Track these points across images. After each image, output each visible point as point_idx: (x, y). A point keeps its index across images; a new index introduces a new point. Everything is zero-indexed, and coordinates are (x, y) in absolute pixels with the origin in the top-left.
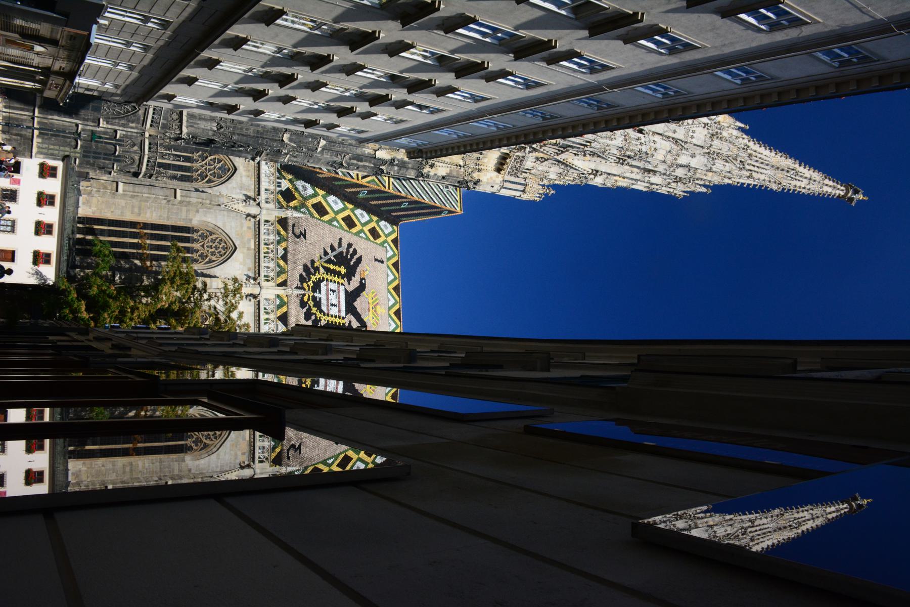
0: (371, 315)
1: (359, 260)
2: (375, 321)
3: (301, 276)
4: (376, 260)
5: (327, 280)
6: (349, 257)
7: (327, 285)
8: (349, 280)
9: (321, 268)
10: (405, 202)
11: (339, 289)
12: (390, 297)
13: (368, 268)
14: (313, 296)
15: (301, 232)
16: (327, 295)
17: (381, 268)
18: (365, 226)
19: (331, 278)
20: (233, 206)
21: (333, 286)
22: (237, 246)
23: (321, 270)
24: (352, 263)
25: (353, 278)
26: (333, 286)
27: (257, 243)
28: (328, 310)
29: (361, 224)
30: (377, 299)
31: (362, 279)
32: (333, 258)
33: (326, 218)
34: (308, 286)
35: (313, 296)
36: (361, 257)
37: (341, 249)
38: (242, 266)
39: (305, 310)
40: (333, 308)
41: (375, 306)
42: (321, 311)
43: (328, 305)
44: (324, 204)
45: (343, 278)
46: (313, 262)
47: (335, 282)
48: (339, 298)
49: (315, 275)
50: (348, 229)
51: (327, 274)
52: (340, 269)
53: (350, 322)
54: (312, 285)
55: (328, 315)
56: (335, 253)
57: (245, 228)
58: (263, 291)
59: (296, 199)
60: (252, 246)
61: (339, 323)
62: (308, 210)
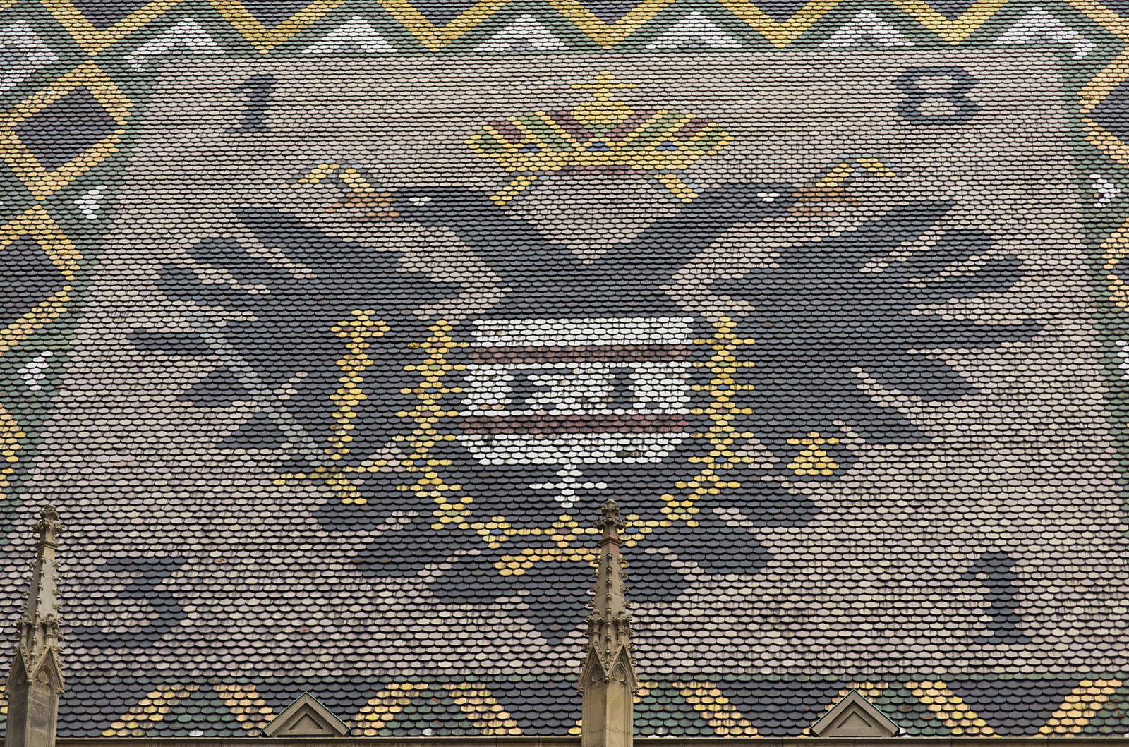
0: (648, 158)
2: (684, 135)
3: (445, 592)
4: (254, 121)
5: (444, 426)
6: (257, 289)
7: (487, 427)
9: (371, 466)
11: (505, 355)
12: (499, 42)
13: (318, 173)
14: (576, 513)
15: (129, 593)
16: (554, 426)
23: (383, 461)
28: (663, 424)
30: (527, 115)
31: (407, 213)
32: (287, 391)
34: (514, 546)
35: (576, 513)
36: (244, 215)
39: (690, 570)
40: (644, 391)
41: (580, 133)
42: (678, 465)
43: (632, 425)
45: (423, 331)
48: (565, 353)
49: (431, 504)
51: (408, 427)
53: (718, 287)
54: (499, 522)
56: (250, 378)
61: (741, 353)
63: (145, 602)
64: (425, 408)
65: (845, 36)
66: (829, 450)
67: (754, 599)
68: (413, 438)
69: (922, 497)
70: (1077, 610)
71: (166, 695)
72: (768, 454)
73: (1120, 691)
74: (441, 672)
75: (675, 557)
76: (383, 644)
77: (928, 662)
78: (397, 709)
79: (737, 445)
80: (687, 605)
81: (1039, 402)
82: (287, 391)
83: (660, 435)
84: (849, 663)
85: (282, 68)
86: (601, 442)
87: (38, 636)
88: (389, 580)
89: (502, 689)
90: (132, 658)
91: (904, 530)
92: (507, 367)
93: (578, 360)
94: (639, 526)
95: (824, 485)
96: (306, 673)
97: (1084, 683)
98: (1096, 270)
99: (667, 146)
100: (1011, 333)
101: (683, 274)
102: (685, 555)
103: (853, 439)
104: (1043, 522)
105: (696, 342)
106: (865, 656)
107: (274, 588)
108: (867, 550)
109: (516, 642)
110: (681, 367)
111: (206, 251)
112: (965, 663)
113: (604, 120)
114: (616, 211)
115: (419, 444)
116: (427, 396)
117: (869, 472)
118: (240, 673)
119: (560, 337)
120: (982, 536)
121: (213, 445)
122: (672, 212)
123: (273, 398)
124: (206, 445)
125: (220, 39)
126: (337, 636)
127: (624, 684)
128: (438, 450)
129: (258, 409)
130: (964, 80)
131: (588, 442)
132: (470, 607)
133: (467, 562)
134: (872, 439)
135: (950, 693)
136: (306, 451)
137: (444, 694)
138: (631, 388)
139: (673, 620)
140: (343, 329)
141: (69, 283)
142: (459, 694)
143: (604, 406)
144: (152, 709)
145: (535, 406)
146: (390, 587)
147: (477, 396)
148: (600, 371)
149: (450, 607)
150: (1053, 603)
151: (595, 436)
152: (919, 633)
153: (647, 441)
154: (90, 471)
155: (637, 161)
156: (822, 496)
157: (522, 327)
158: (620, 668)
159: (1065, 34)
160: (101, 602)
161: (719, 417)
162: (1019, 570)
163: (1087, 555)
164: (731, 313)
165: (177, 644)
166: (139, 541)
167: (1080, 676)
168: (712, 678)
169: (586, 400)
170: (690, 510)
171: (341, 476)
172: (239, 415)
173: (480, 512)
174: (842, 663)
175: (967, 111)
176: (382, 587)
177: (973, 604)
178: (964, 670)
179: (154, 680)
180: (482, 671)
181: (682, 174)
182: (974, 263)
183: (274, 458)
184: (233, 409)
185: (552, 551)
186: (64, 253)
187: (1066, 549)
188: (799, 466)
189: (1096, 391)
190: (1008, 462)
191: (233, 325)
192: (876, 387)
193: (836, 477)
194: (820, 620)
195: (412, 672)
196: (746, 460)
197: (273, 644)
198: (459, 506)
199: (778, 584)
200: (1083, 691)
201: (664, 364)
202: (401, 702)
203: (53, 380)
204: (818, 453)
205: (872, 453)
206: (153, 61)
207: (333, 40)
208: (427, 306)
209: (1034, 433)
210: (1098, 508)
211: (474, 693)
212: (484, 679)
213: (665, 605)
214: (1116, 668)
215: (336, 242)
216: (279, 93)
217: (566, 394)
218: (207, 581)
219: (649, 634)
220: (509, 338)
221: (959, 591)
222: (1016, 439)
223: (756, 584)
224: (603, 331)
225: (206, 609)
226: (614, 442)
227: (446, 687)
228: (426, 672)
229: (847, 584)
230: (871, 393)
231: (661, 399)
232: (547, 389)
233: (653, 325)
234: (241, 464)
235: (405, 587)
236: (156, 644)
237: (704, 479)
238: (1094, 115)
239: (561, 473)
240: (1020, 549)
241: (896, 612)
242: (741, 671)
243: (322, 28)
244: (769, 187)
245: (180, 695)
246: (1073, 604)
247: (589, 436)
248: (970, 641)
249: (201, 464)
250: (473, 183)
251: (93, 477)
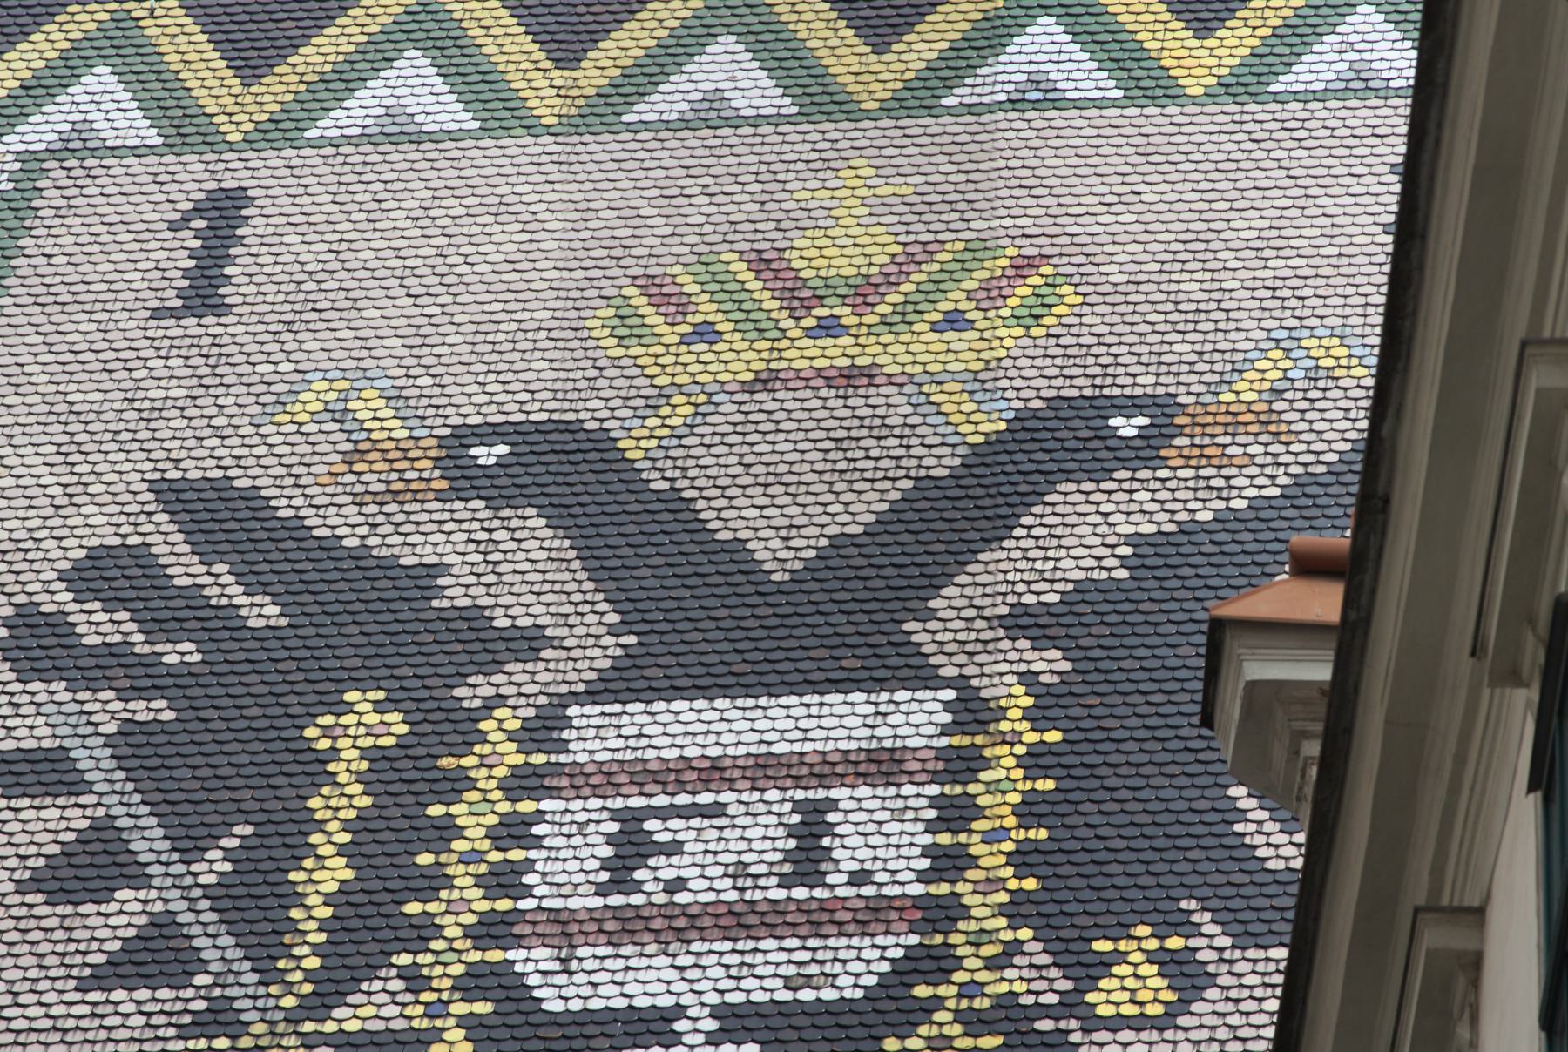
5: (490, 931)
6: (180, 653)
9: (347, 1019)
11: (605, 780)
17: (308, 228)
24: (264, 613)
25: (456, 592)
30: (705, 263)
32: (214, 866)
37: (93, 761)
41: (798, 297)
45: (466, 733)
47: (513, 831)
48: (715, 773)
51: (425, 931)
52: (349, 761)
55: (943, 914)
61: (1034, 761)
64: (456, 894)
66: (1166, 962)
68: (429, 958)
83: (867, 941)
86: (759, 958)
92: (609, 803)
93: (739, 785)
99: (954, 321)
105: (956, 741)
110: (919, 795)
113: (845, 266)
114: (842, 465)
115: (439, 970)
116: (461, 869)
117: (1230, 1007)
119: (712, 739)
121: (72, 984)
122: (942, 464)
123: (188, 880)
124: (59, 985)
131: (736, 959)
138: (826, 842)
140: (327, 732)
143: (774, 881)
148: (775, 808)
151: (750, 945)
153: (842, 955)
155: (889, 353)
157: (646, 719)
161: (978, 899)
164: (1028, 679)
172: (124, 919)
183: (179, 1006)
184: (114, 907)
188: (1106, 999)
191: (129, 729)
193: (1166, 1021)
201: (892, 791)
204: (1142, 970)
205: (1241, 967)
208: (480, 679)
217: (709, 858)
220: (620, 743)
224: (790, 724)
226: (783, 957)
231: (879, 865)
232: (675, 848)
233: (882, 708)
234: (117, 1021)
237: (935, 1031)
239: (680, 1026)
244: (1130, 406)
247: (740, 945)
249: (48, 1023)
250: (591, 412)
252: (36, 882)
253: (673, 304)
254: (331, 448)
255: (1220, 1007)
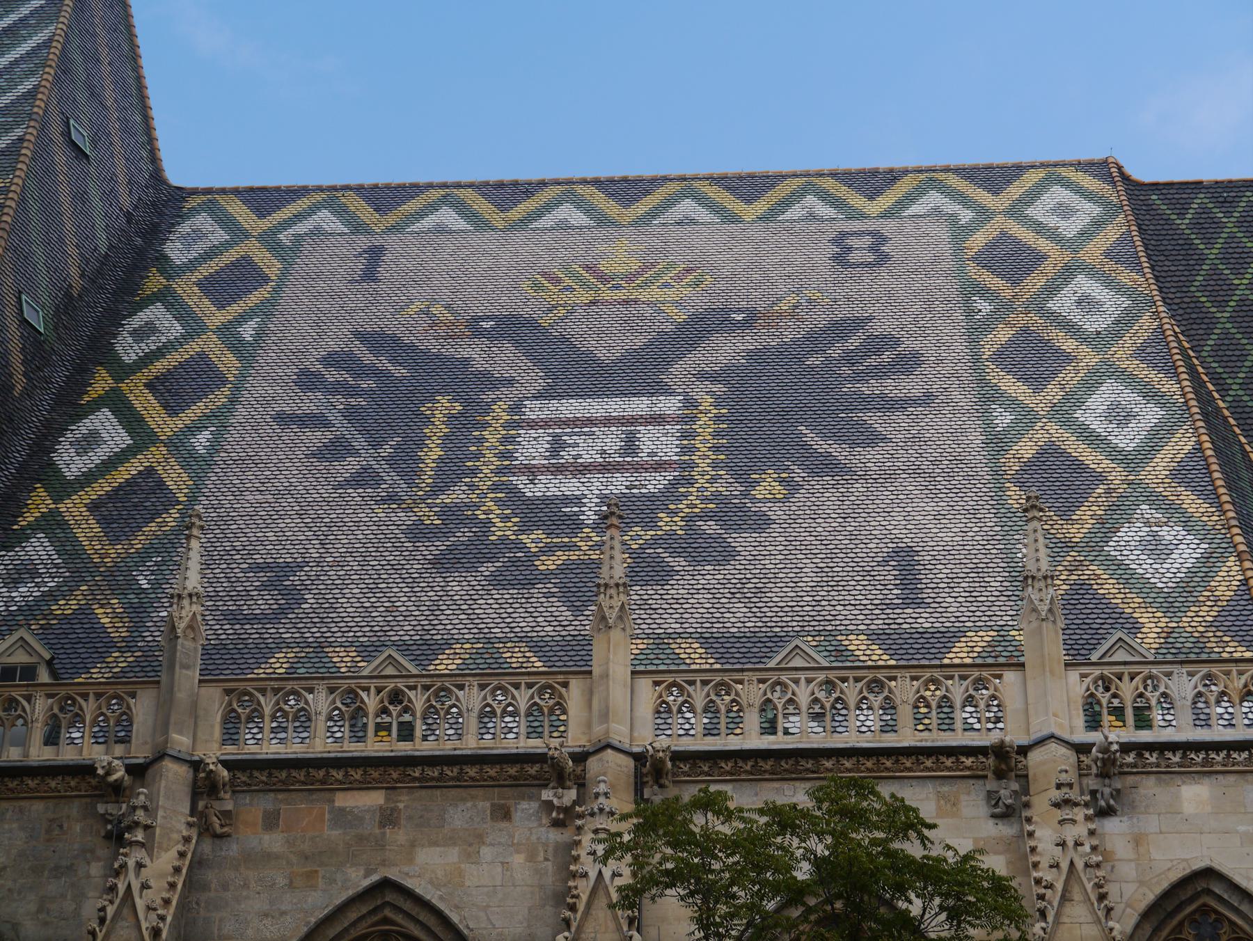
0: (654, 293)
1: (377, 341)
2: (679, 278)
3: (497, 581)
4: (370, 275)
5: (499, 471)
7: (531, 472)
8: (489, 381)
10: (67, 134)
11: (546, 424)
12: (547, 221)
13: (414, 308)
14: (596, 527)
15: (264, 587)
16: (582, 470)
18: (197, 320)
19: (489, 455)
20: (156, 894)
21: (533, 448)
22: (375, 878)
23: (455, 495)
26: (533, 448)
27: (357, 774)
28: (659, 466)
29: (189, 336)
31: (478, 333)
32: (386, 450)
33: (175, 478)
34: (549, 550)
35: (596, 527)
37: (334, 417)
38: (486, 852)
39: (679, 563)
41: (604, 279)
43: (638, 468)
44: (102, 488)
45: (487, 409)
46: (418, 532)
48: (590, 422)
50: (226, 391)
51: (474, 472)
53: (702, 376)
56: (359, 442)
57: (273, 841)
58: (619, 732)
59: (85, 613)
60: (374, 799)
61: (718, 419)
62: (145, 555)
63: (276, 592)
65: (795, 212)
66: (782, 481)
67: (725, 581)
68: (477, 479)
69: (849, 511)
70: (963, 585)
71: (288, 655)
72: (736, 485)
73: (995, 639)
74: (492, 635)
75: (667, 555)
76: (450, 617)
77: (853, 622)
78: (460, 661)
79: (713, 480)
80: (676, 587)
81: (935, 447)
82: (386, 450)
84: (795, 624)
85: (391, 241)
87: (186, 602)
88: (456, 574)
89: (538, 646)
90: (264, 631)
91: (836, 533)
94: (639, 535)
95: (777, 504)
96: (393, 638)
97: (969, 634)
98: (976, 359)
99: (666, 285)
100: (915, 402)
101: (676, 369)
102: (675, 553)
103: (798, 473)
104: (938, 526)
106: (807, 618)
107: (371, 581)
108: (809, 547)
109: (549, 614)
111: (331, 360)
112: (881, 622)
113: (621, 269)
118: (344, 639)
120: (893, 536)
125: (347, 223)
126: (417, 613)
127: (624, 629)
128: (495, 488)
129: (365, 463)
130: (880, 239)
132: (516, 591)
133: (514, 562)
134: (813, 473)
135: (870, 642)
136: (399, 490)
137: (495, 650)
138: (637, 443)
139: (665, 597)
141: (231, 382)
142: (506, 650)
144: (278, 665)
145: (566, 456)
146: (457, 579)
147: (525, 451)
149: (501, 592)
150: (946, 580)
152: (847, 602)
154: (239, 506)
155: (644, 295)
156: (776, 512)
158: (620, 618)
159: (951, 207)
160: (244, 593)
162: (921, 558)
163: (971, 548)
165: (298, 621)
166: (273, 551)
167: (966, 629)
168: (693, 636)
169: (604, 452)
170: (679, 523)
171: (423, 505)
173: (524, 528)
174: (790, 624)
175: (883, 259)
176: (451, 579)
177: (886, 582)
178: (880, 627)
179: (281, 644)
180: (523, 634)
181: (677, 304)
182: (886, 356)
184: (346, 463)
185: (577, 553)
186: (228, 363)
187: (955, 543)
188: (759, 492)
189: (976, 439)
190: (911, 486)
192: (816, 439)
193: (785, 499)
194: (774, 595)
195: (472, 636)
196: (720, 489)
197: (369, 619)
198: (509, 524)
199: (743, 572)
200: (969, 639)
202: (462, 656)
203: (215, 446)
206: (298, 239)
207: (428, 222)
209: (931, 467)
210: (978, 516)
211: (517, 649)
212: (524, 640)
213: (659, 587)
214: (993, 623)
215: (426, 353)
216: (388, 257)
218: (322, 578)
219: (647, 607)
221: (876, 573)
222: (918, 471)
223: (726, 572)
225: (321, 596)
227: (496, 645)
228: (482, 636)
229: (794, 570)
230: (812, 443)
235: (468, 579)
236: (283, 621)
238: (973, 259)
240: (921, 544)
241: (830, 589)
242: (715, 630)
243: (420, 215)
244: (739, 311)
245: (299, 655)
246: (961, 580)
248: (884, 607)
250: (525, 312)
251: (242, 510)
252: (314, 455)
253: (556, 281)
254: (424, 322)
255: (807, 495)
